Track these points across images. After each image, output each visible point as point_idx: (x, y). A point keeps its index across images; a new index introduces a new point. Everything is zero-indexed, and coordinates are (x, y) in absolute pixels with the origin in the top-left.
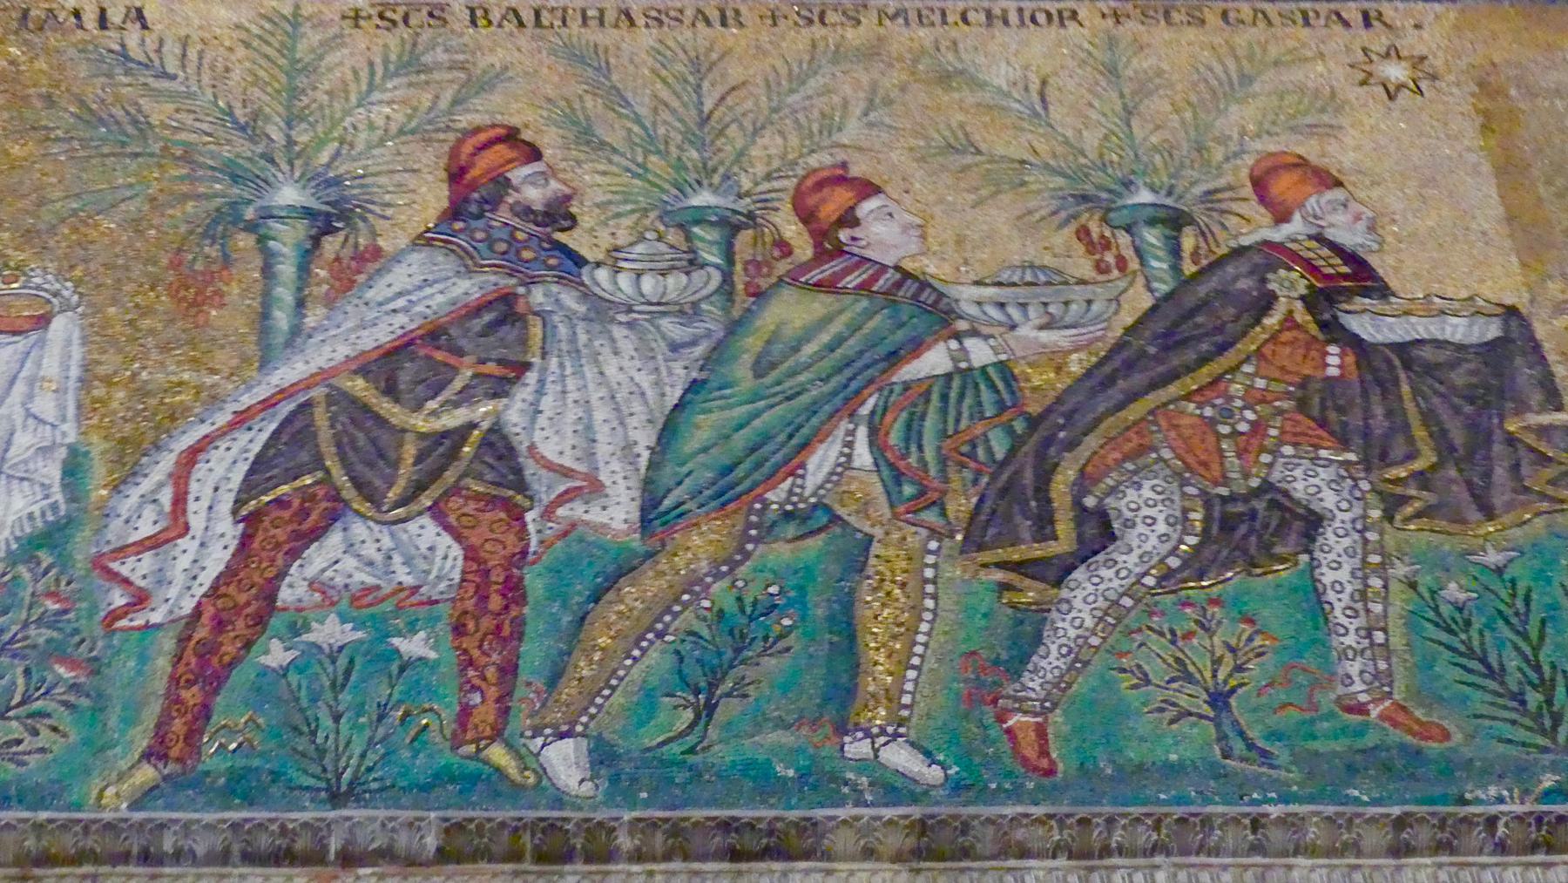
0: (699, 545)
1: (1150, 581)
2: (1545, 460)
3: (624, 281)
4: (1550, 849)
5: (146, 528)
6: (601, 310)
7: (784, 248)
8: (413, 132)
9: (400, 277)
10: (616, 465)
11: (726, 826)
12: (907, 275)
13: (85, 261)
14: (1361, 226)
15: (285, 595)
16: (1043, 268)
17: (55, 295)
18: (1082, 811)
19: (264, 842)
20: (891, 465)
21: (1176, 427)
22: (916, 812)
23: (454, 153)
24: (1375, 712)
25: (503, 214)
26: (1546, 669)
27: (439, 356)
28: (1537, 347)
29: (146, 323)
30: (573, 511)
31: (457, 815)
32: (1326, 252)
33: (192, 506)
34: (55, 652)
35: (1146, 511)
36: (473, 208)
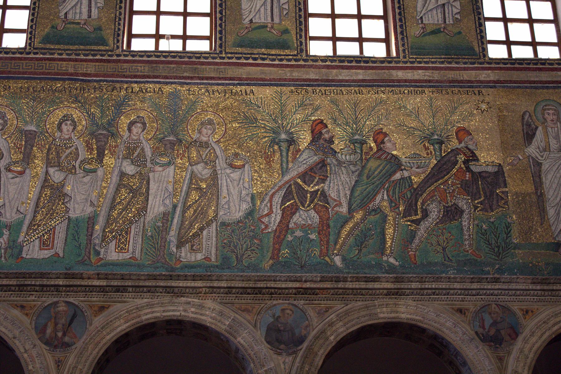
0: (358, 216)
1: (434, 224)
2: (502, 199)
3: (343, 157)
4: (496, 282)
5: (266, 212)
6: (340, 163)
7: (371, 148)
8: (304, 121)
9: (305, 156)
10: (344, 199)
11: (365, 277)
12: (393, 155)
13: (249, 152)
14: (474, 145)
15: (290, 226)
16: (417, 154)
17: (245, 159)
18: (422, 276)
19: (293, 279)
20: (391, 199)
21: (439, 191)
22: (395, 275)
23: (312, 126)
24: (470, 252)
25: (321, 141)
26: (499, 243)
27: (312, 174)
28: (504, 173)
29: (261, 166)
30: (336, 209)
31: (323, 275)
32: (468, 151)
33: (273, 207)
34: (254, 237)
35: (434, 209)
36: (316, 139)
